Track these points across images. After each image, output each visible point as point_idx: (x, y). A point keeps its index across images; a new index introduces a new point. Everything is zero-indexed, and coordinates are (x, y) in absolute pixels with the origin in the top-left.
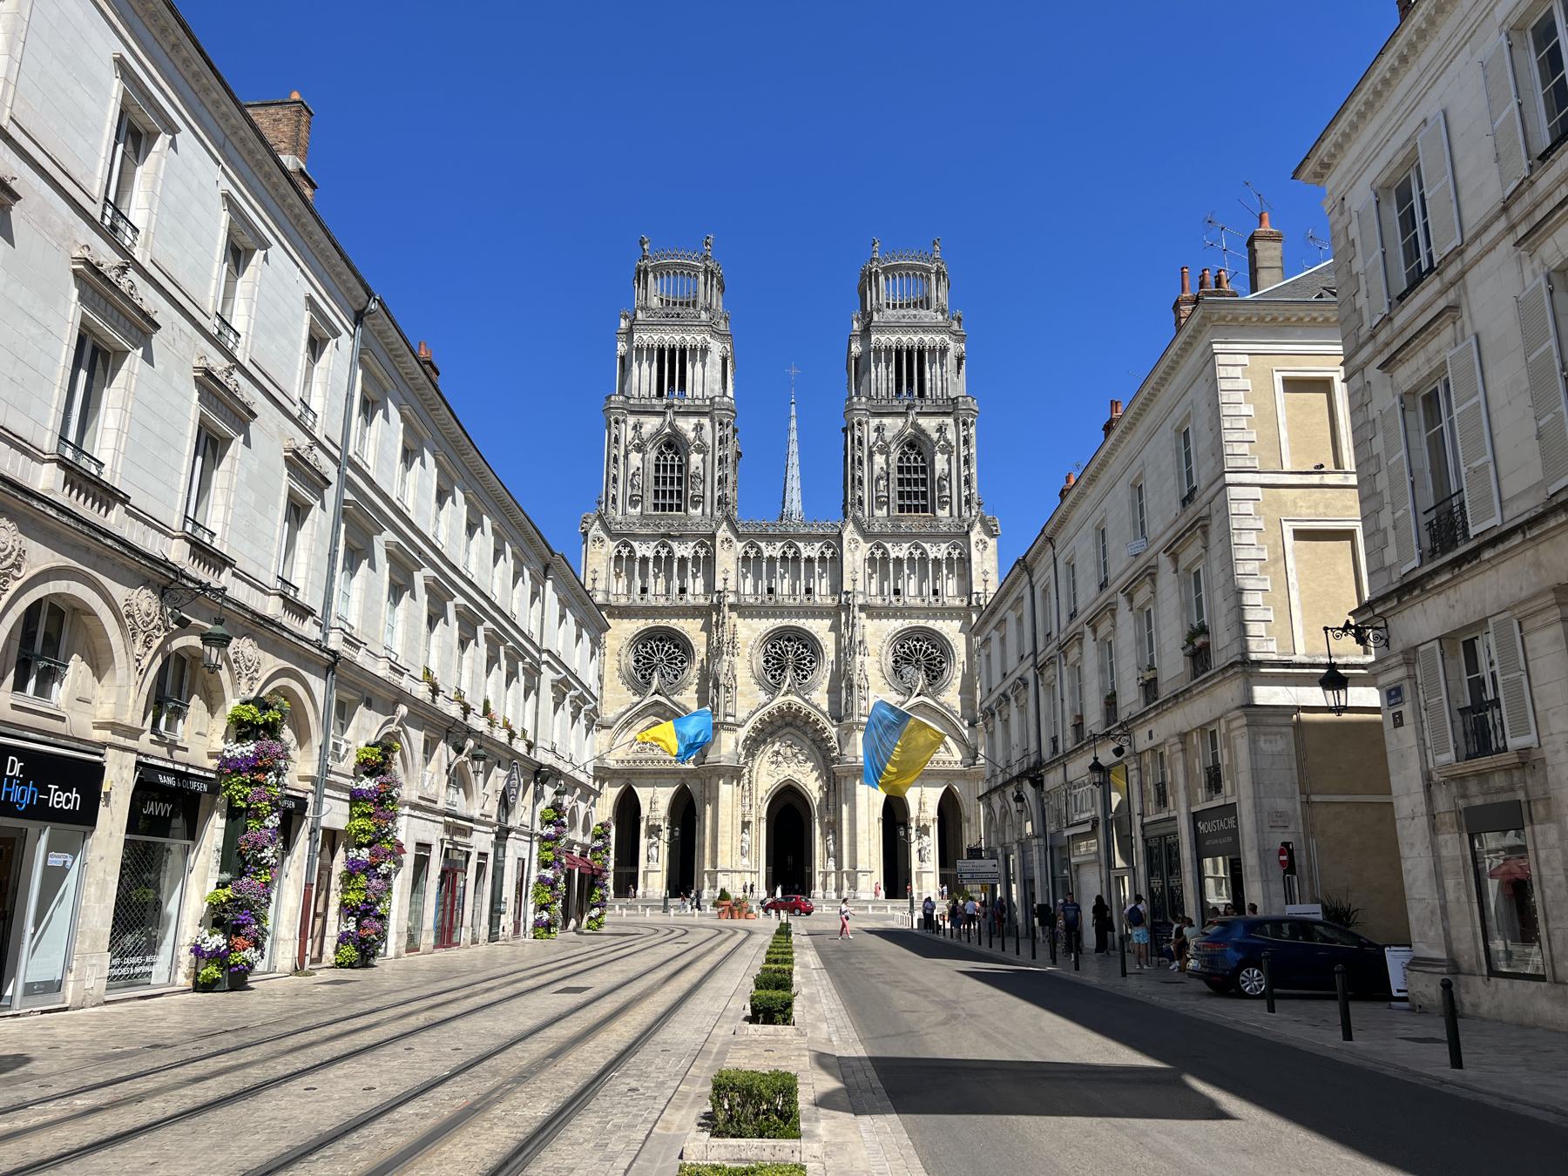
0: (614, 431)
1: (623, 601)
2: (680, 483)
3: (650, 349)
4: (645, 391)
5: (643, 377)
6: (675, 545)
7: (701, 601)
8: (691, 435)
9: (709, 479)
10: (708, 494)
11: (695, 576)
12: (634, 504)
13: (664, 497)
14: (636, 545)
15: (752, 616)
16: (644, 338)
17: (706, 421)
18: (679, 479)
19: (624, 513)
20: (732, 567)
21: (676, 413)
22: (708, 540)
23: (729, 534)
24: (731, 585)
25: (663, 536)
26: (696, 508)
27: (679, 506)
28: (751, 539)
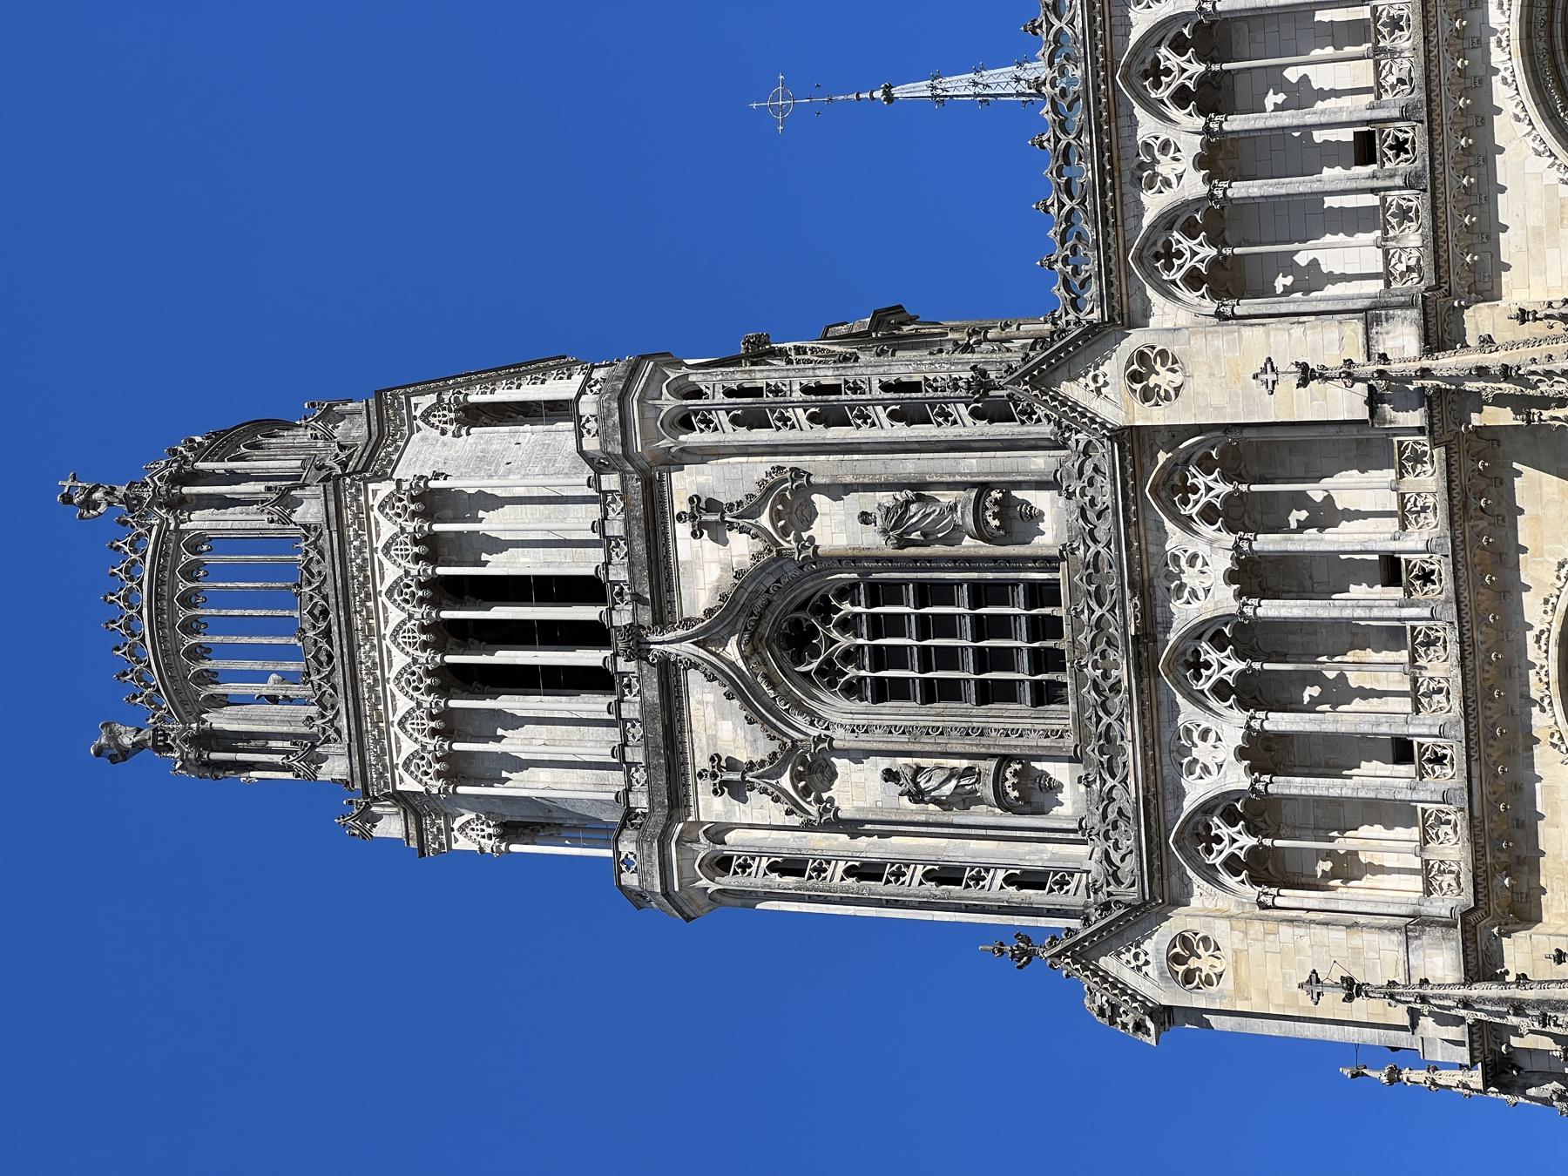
0: (758, 878)
1: (1453, 849)
2: (944, 593)
3: (449, 726)
4: (597, 745)
5: (559, 751)
6: (1185, 614)
7: (1428, 481)
8: (741, 549)
9: (909, 466)
10: (971, 465)
11: (1326, 516)
12: (1033, 795)
13: (1004, 659)
14: (1196, 791)
15: (1488, 232)
16: (408, 748)
17: (684, 485)
18: (928, 593)
19: (1080, 833)
20: (1257, 342)
21: (662, 619)
22: (1151, 467)
23: (1113, 368)
24: (1334, 343)
25: (1144, 665)
26: (1034, 517)
27: (1043, 594)
28: (1126, 269)
